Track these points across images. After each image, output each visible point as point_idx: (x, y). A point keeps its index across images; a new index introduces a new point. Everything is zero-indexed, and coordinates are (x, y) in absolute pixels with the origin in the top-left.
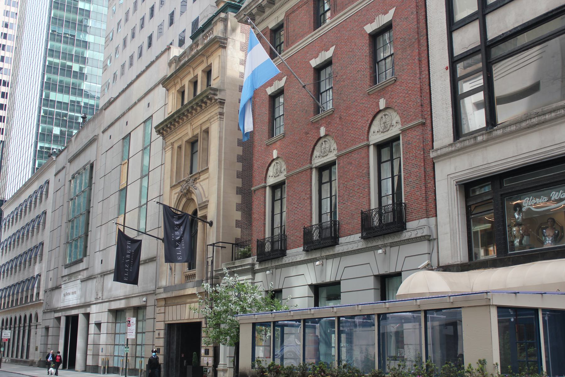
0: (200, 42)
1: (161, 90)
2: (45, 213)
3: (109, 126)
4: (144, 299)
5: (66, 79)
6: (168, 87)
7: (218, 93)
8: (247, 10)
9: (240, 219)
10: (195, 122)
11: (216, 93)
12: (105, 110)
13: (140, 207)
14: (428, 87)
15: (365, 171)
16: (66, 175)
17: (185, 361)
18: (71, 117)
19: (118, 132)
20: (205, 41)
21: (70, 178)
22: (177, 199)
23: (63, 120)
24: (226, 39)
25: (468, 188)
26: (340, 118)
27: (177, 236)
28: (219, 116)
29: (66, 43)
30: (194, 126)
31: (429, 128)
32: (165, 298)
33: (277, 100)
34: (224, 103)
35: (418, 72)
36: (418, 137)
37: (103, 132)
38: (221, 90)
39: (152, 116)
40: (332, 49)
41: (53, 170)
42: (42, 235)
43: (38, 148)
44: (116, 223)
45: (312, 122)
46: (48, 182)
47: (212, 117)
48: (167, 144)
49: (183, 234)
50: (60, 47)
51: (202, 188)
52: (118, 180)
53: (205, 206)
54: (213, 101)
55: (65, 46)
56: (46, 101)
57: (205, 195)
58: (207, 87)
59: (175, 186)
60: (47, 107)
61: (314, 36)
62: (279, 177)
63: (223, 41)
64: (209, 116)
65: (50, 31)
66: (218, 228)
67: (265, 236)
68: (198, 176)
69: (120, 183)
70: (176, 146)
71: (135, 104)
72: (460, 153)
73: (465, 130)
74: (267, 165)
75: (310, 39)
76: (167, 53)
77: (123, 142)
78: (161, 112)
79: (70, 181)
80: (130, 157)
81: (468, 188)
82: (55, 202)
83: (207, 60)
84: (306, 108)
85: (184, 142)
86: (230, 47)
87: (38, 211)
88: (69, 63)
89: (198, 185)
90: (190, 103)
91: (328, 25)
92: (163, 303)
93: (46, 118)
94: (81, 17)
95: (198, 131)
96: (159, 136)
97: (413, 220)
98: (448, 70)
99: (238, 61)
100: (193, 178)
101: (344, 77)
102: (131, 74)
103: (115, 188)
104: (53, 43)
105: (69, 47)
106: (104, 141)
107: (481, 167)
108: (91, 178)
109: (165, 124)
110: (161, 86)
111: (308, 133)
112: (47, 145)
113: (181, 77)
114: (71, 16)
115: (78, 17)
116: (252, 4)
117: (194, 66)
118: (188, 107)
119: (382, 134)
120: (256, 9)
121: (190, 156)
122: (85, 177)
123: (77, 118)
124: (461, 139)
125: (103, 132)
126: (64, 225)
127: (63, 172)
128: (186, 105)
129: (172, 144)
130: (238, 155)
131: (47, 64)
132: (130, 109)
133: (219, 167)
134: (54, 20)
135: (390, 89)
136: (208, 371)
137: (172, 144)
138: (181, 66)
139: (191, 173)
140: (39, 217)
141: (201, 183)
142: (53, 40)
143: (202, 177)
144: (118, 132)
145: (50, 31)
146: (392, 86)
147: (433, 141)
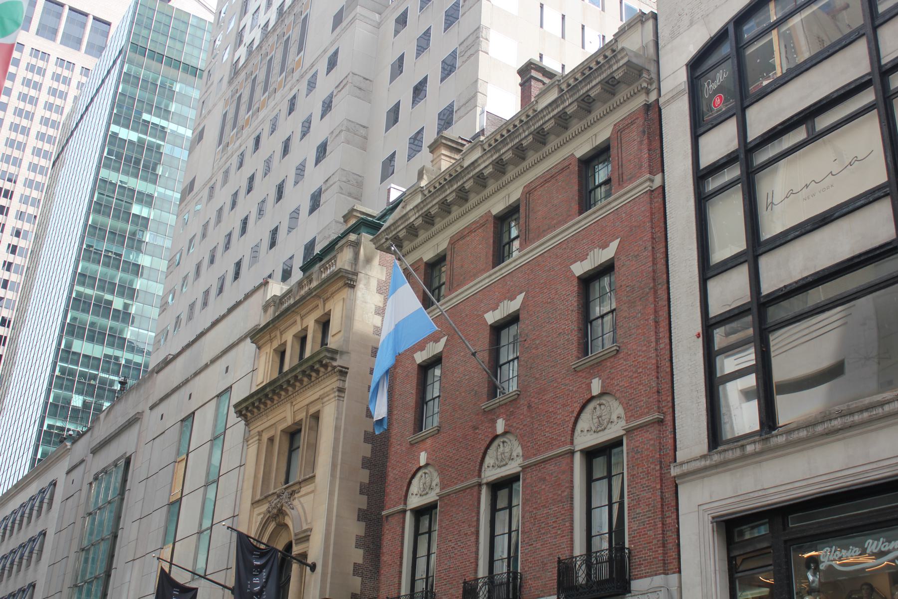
0: (314, 276)
1: (248, 346)
2: (43, 534)
3: (162, 400)
5: (101, 321)
6: (261, 343)
7: (338, 357)
8: (392, 232)
9: (360, 561)
11: (335, 356)
12: (157, 373)
13: (200, 533)
14: (668, 364)
15: (566, 493)
16: (84, 473)
18: (103, 381)
19: (174, 409)
20: (323, 276)
21: (91, 479)
22: (260, 523)
23: (89, 384)
24: (356, 274)
25: (731, 528)
26: (529, 407)
27: (256, 585)
28: (337, 394)
29: (107, 265)
30: (296, 408)
31: (670, 429)
33: (430, 372)
34: (347, 373)
35: (653, 339)
36: (652, 442)
37: (151, 408)
38: (342, 353)
39: (231, 387)
40: (520, 298)
41: (65, 464)
42: (35, 570)
43: (45, 428)
44: (158, 558)
45: (484, 411)
46: (54, 484)
48: (252, 433)
49: (266, 582)
50: (97, 271)
51: (303, 507)
52: (169, 486)
53: (305, 538)
54: (330, 369)
55: (105, 270)
56: (65, 354)
57: (306, 520)
59: (259, 501)
60: (67, 362)
61: (493, 277)
62: (428, 496)
63: (350, 276)
64: (321, 392)
65: (85, 246)
66: (324, 574)
67: (399, 593)
68: (296, 488)
69: (171, 492)
70: (265, 437)
71: (206, 366)
72: (718, 470)
73: (727, 434)
74: (410, 476)
75: (487, 281)
76: (261, 291)
77: (182, 425)
78: (245, 382)
79: (91, 484)
80: (191, 450)
81: (731, 528)
82: (61, 517)
83: (324, 304)
84: (476, 388)
85: (279, 433)
86: (361, 286)
87: (32, 531)
88: (108, 297)
89: (296, 502)
90: (292, 370)
91: (515, 261)
93: (62, 380)
94: (134, 228)
95: (302, 415)
96: (240, 419)
97: (639, 578)
98: (701, 339)
99: (373, 309)
100: (290, 490)
101: (537, 342)
102: (204, 319)
103: (162, 499)
104: (87, 264)
105: (110, 271)
106: (152, 423)
107: (752, 495)
108: (125, 480)
109: (251, 401)
110: (249, 340)
111: (477, 428)
112: (59, 424)
113: (282, 328)
114: (120, 225)
115: (129, 227)
116: (400, 223)
117: (303, 313)
118: (289, 376)
119: (595, 435)
120: (405, 230)
121: (287, 454)
122: (115, 479)
123: (112, 383)
124: (720, 448)
125: (151, 408)
126: (73, 556)
127: (81, 469)
128: (287, 373)
129: (260, 434)
130: (364, 458)
131: (74, 295)
132: (196, 374)
133: (333, 475)
134: (92, 230)
135: (608, 364)
137: (260, 434)
138: (283, 311)
139: (287, 482)
140: (32, 540)
141: (302, 499)
142: (87, 259)
143: (304, 490)
144: (174, 409)
145: (85, 246)
146: (612, 360)
147: (675, 450)
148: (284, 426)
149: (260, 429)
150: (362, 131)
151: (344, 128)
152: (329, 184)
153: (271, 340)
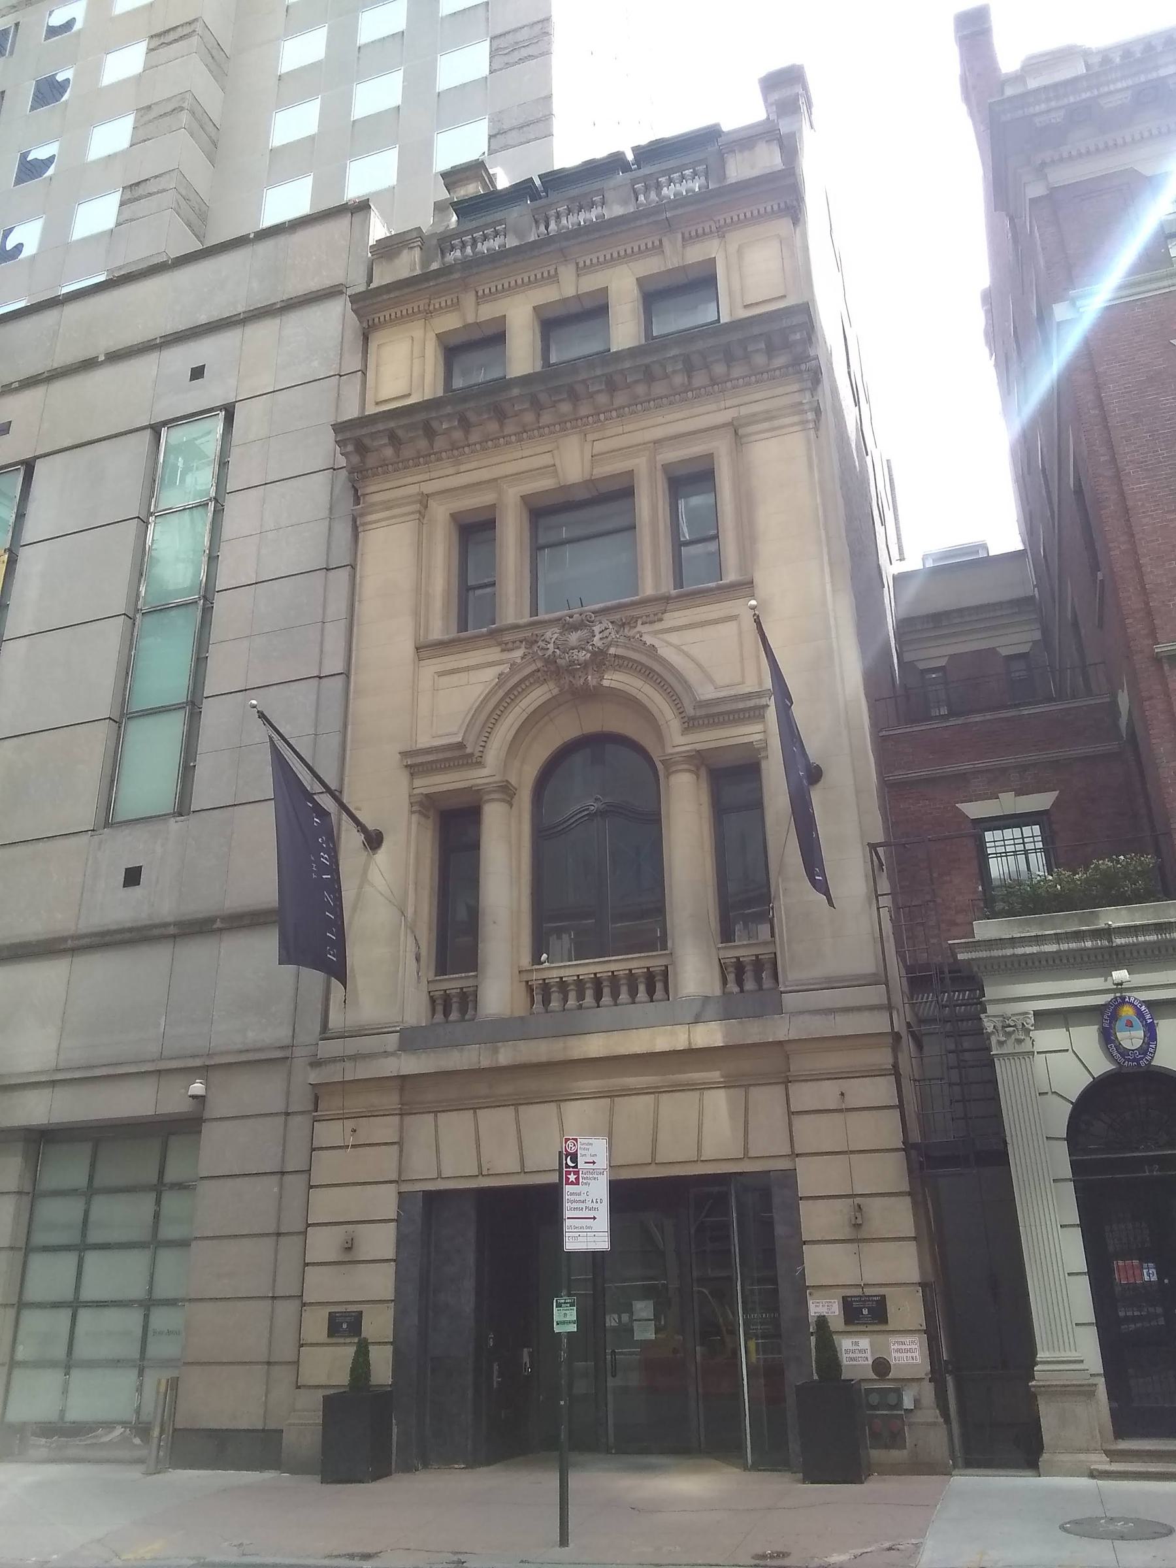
4: (197, 1088)
10: (608, 433)
17: (496, 1367)
22: (499, 685)
30: (599, 447)
32: (403, 1080)
39: (229, 412)
47: (769, 416)
54: (780, 361)
57: (712, 681)
58: (647, 339)
68: (650, 610)
70: (440, 512)
71: (89, 364)
83: (684, 247)
92: (391, 1100)
95: (640, 463)
96: (342, 461)
100: (616, 617)
109: (422, 416)
129: (424, 500)
136: (908, 1403)
137: (424, 500)
141: (673, 638)
143: (675, 618)
148: (545, 483)
149: (428, 488)
150: (210, 128)
151: (185, 105)
152: (140, 191)
153: (428, 314)
